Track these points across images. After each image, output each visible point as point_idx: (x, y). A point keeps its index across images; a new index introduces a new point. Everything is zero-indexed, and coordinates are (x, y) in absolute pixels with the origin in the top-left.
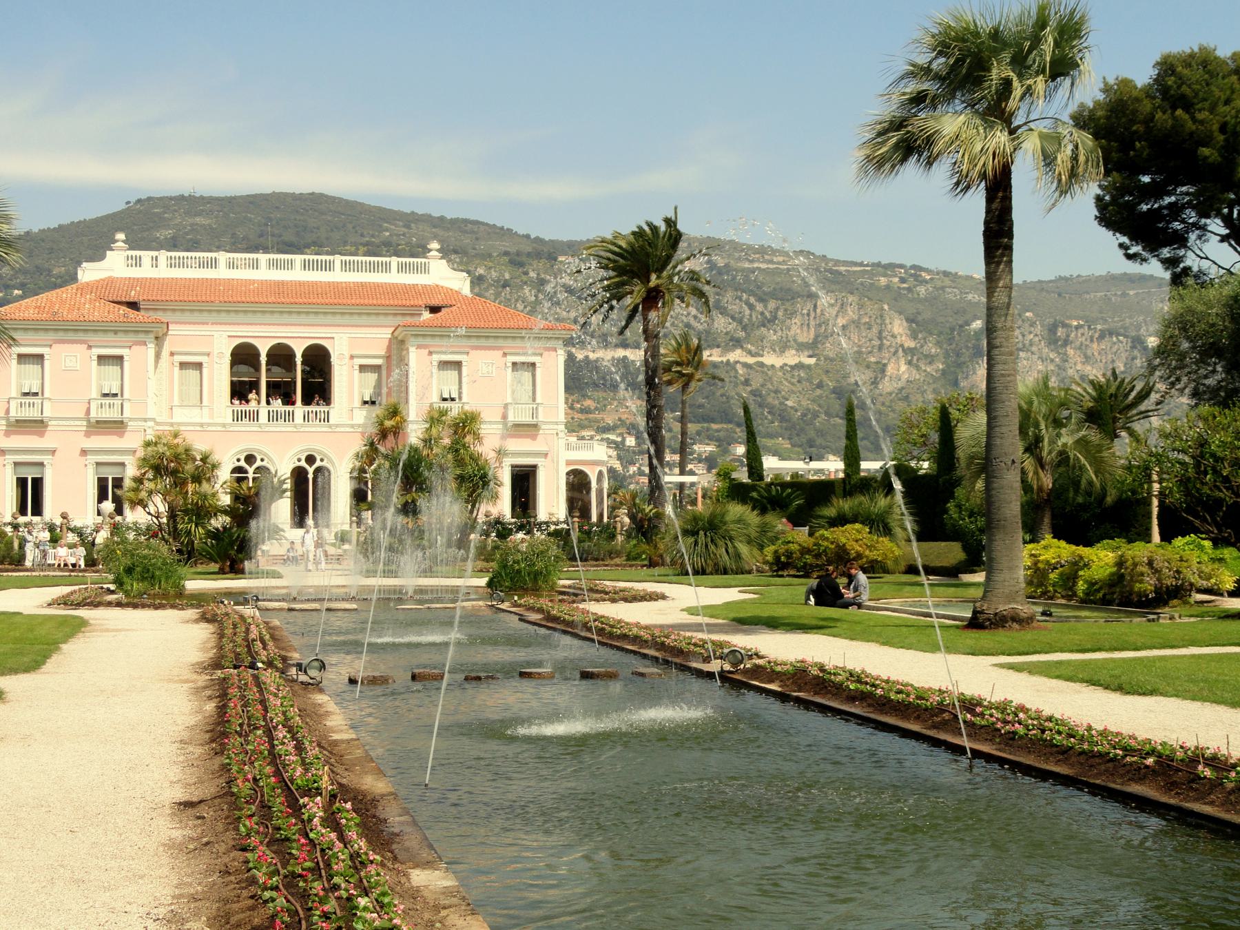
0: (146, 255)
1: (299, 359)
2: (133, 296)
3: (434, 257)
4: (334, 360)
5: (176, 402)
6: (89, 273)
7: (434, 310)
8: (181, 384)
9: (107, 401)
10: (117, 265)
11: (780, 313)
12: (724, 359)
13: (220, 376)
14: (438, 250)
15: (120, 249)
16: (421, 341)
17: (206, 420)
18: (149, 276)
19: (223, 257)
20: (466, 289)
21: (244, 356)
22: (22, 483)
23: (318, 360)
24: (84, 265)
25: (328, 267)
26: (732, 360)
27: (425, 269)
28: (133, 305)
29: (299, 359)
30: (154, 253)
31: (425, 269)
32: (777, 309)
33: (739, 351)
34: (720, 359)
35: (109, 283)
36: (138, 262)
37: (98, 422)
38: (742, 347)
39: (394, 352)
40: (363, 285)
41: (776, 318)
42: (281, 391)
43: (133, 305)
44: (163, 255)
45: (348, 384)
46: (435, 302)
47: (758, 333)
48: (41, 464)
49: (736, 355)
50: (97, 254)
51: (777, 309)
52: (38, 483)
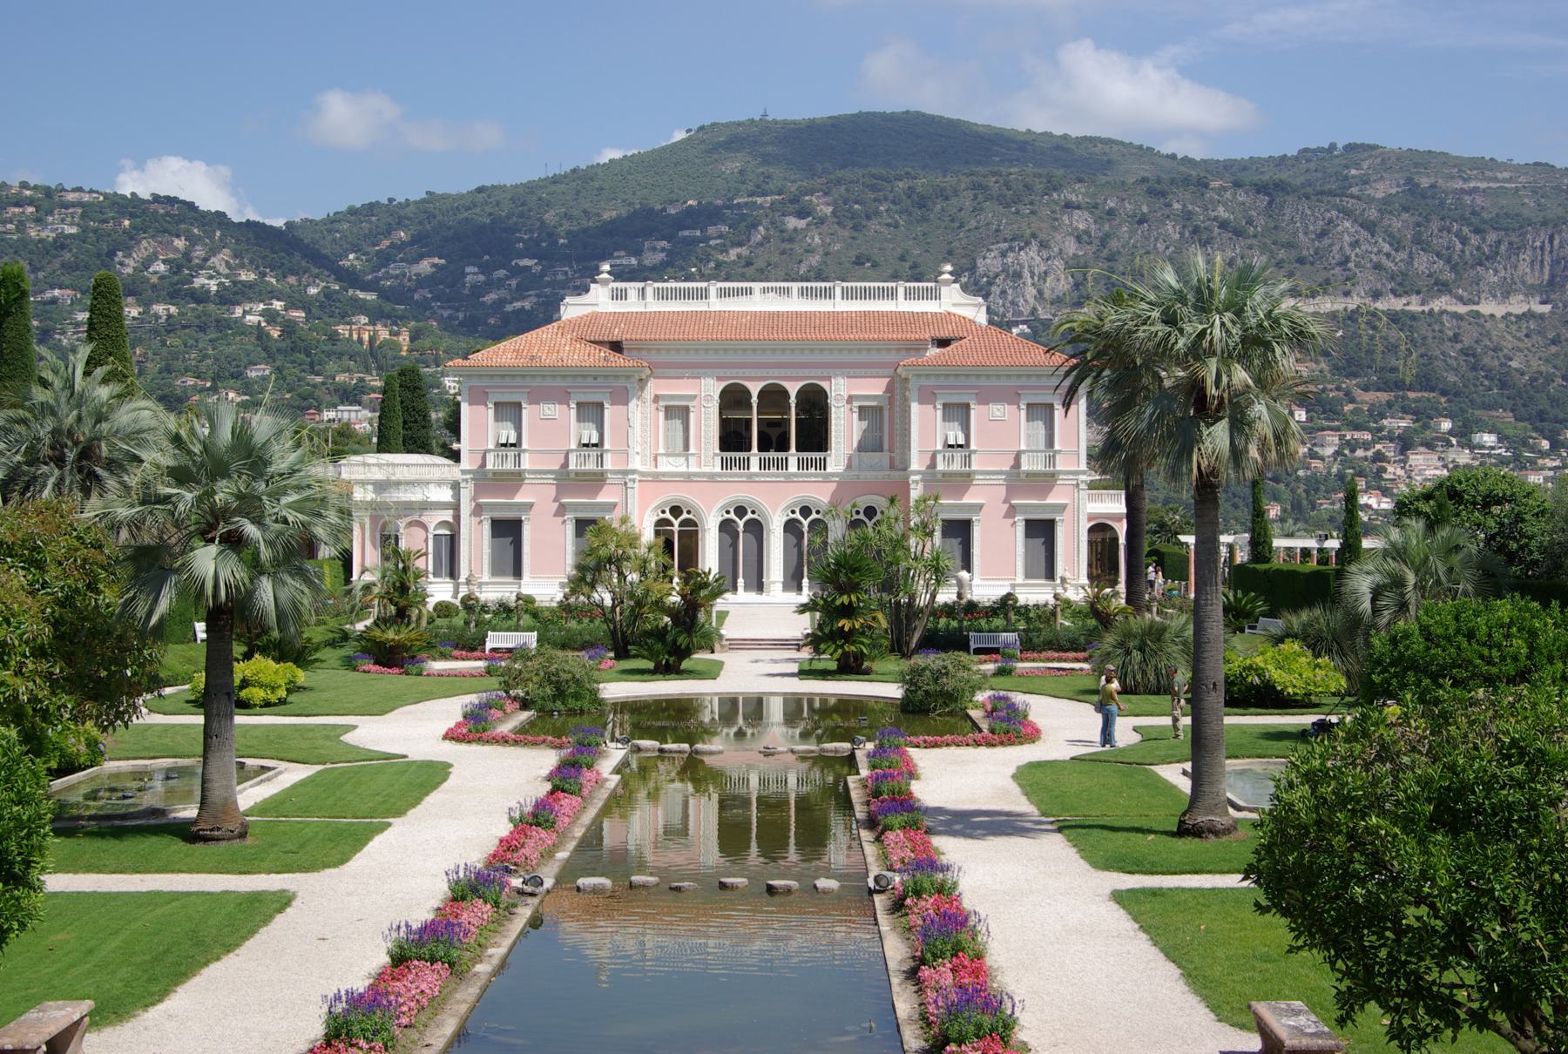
0: (633, 287)
1: (793, 400)
2: (616, 335)
3: (947, 283)
4: (832, 401)
5: (661, 451)
7: (943, 343)
8: (667, 430)
9: (585, 451)
10: (600, 301)
11: (1503, 248)
12: (1426, 308)
13: (706, 423)
14: (951, 273)
15: (605, 282)
17: (693, 469)
18: (635, 310)
19: (714, 287)
20: (982, 318)
21: (733, 398)
23: (815, 406)
24: (568, 300)
25: (828, 294)
26: (1436, 309)
27: (935, 295)
28: (616, 347)
29: (793, 400)
30: (641, 285)
31: (937, 297)
32: (1499, 242)
33: (1443, 299)
34: (1420, 309)
35: (594, 318)
36: (620, 295)
37: (577, 474)
38: (1450, 292)
39: (898, 391)
41: (1497, 253)
42: (773, 440)
43: (616, 347)
45: (845, 429)
46: (944, 334)
47: (1472, 273)
49: (1440, 304)
51: (1499, 242)
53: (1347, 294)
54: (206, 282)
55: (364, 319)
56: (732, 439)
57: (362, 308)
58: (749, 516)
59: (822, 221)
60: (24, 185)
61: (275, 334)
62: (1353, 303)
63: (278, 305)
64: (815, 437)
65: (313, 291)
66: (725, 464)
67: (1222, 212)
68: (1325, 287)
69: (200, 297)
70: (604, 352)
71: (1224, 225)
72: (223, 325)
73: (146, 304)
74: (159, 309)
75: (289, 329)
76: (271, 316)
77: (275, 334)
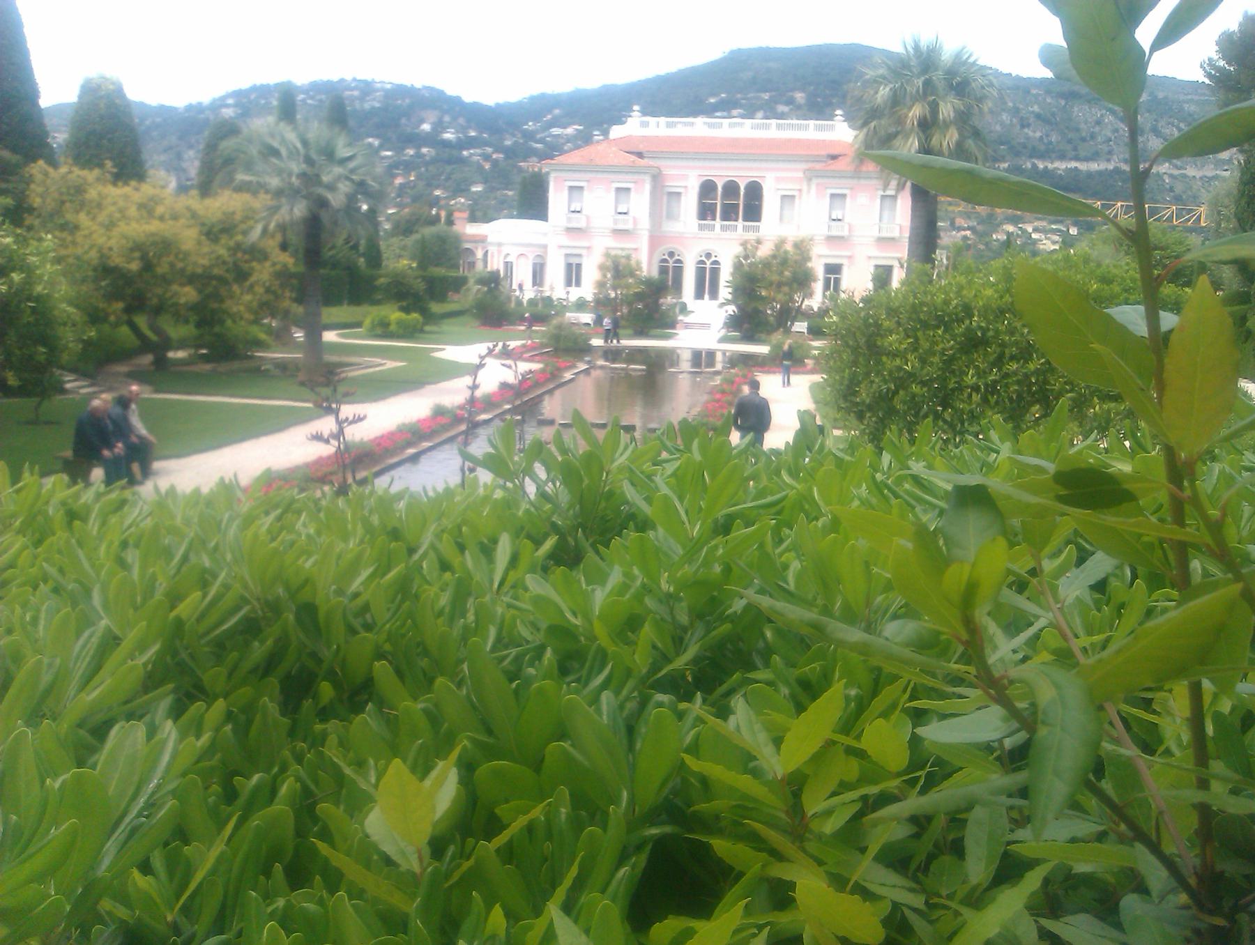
0: (652, 120)
2: (641, 148)
6: (616, 132)
7: (834, 157)
16: (820, 180)
21: (707, 188)
22: (569, 266)
27: (832, 128)
28: (640, 155)
40: (789, 140)
42: (729, 213)
43: (640, 155)
44: (663, 120)
46: (836, 152)
48: (580, 256)
50: (619, 120)
52: (579, 266)
53: (1108, 160)
54: (449, 136)
55: (535, 159)
56: (706, 212)
57: (534, 152)
58: (713, 259)
59: (799, 107)
60: (354, 80)
61: (487, 166)
62: (1111, 167)
63: (489, 150)
64: (753, 212)
65: (508, 143)
66: (701, 227)
67: (1036, 108)
68: (1094, 157)
69: (446, 144)
70: (633, 158)
71: (1038, 116)
72: (463, 161)
73: (419, 147)
74: (425, 150)
75: (495, 163)
76: (487, 158)
77: (487, 166)
